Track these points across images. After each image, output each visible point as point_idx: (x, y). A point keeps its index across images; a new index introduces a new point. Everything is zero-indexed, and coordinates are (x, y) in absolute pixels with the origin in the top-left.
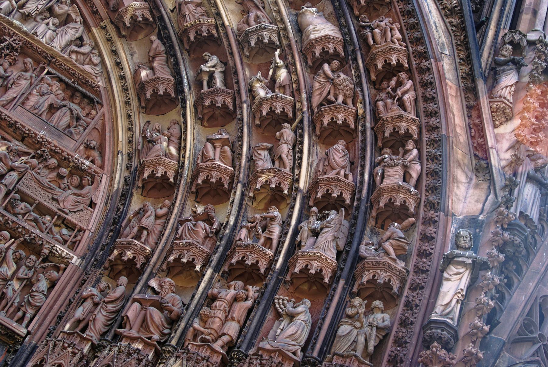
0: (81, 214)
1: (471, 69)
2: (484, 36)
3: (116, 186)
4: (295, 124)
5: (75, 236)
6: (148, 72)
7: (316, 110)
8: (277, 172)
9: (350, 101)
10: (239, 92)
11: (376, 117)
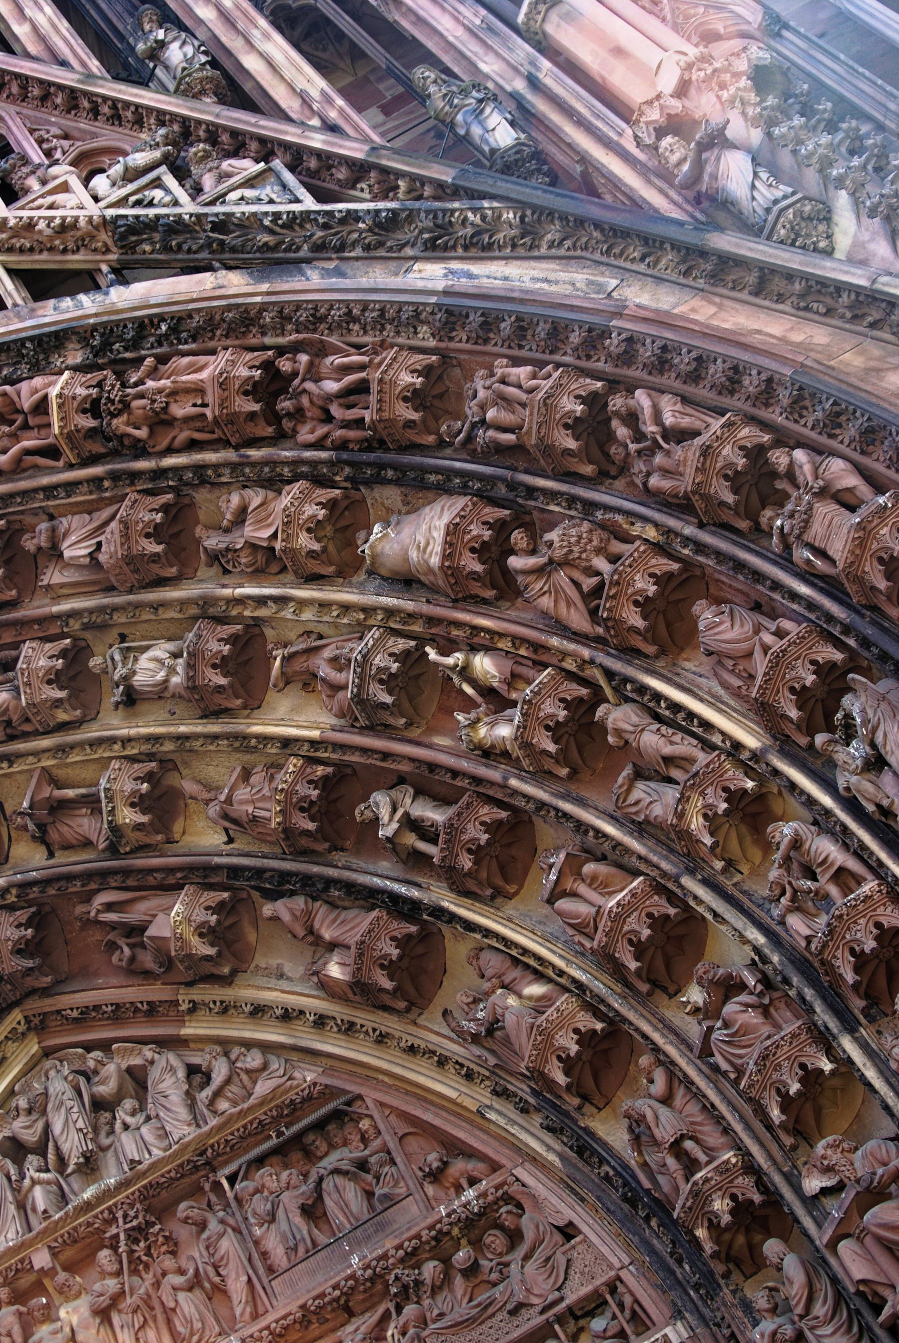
0: (577, 1266)
1: (676, 246)
2: (615, 183)
3: (552, 1157)
4: (608, 692)
5: (621, 1306)
6: (336, 957)
7: (600, 630)
8: (697, 783)
9: (617, 547)
10: (477, 780)
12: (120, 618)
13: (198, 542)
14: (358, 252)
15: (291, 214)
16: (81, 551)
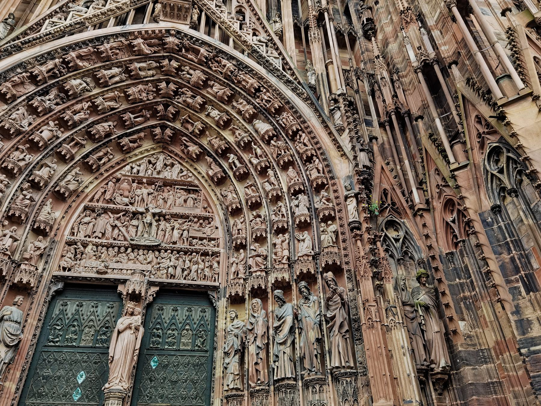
1: (323, 118)
2: (322, 100)
6: (211, 171)
9: (286, 151)
10: (246, 164)
11: (298, 153)
13: (232, 102)
14: (282, 81)
16: (216, 91)
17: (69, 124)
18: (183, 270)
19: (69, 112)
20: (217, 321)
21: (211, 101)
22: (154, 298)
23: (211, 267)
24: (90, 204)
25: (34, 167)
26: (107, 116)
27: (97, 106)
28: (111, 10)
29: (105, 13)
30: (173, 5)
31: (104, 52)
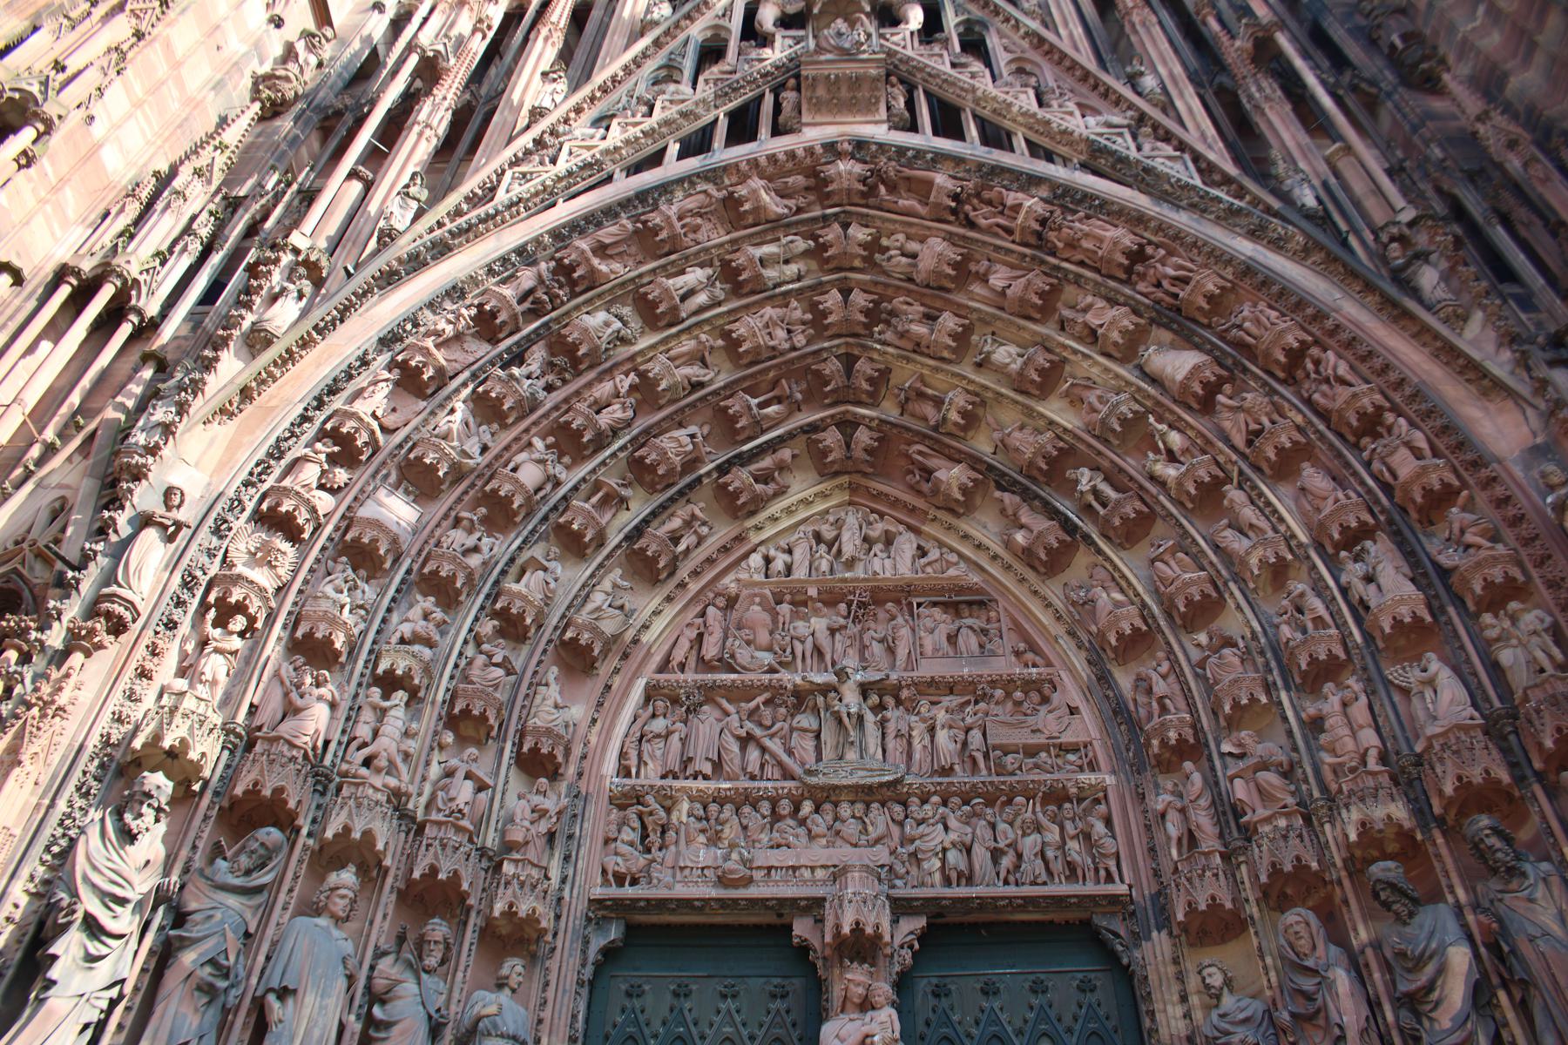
0: (1073, 727)
1: (1383, 295)
7: (1247, 451)
8: (1265, 543)
9: (1276, 417)
10: (1141, 487)
11: (1324, 415)
12: (998, 324)
14: (1212, 217)
15: (1187, 185)
17: (585, 440)
18: (996, 855)
19: (582, 406)
20: (1152, 1014)
21: (985, 321)
22: (914, 954)
23: (1087, 836)
24: (662, 677)
25: (503, 572)
26: (682, 410)
27: (656, 382)
28: (667, 123)
29: (653, 130)
30: (837, 76)
31: (662, 229)
